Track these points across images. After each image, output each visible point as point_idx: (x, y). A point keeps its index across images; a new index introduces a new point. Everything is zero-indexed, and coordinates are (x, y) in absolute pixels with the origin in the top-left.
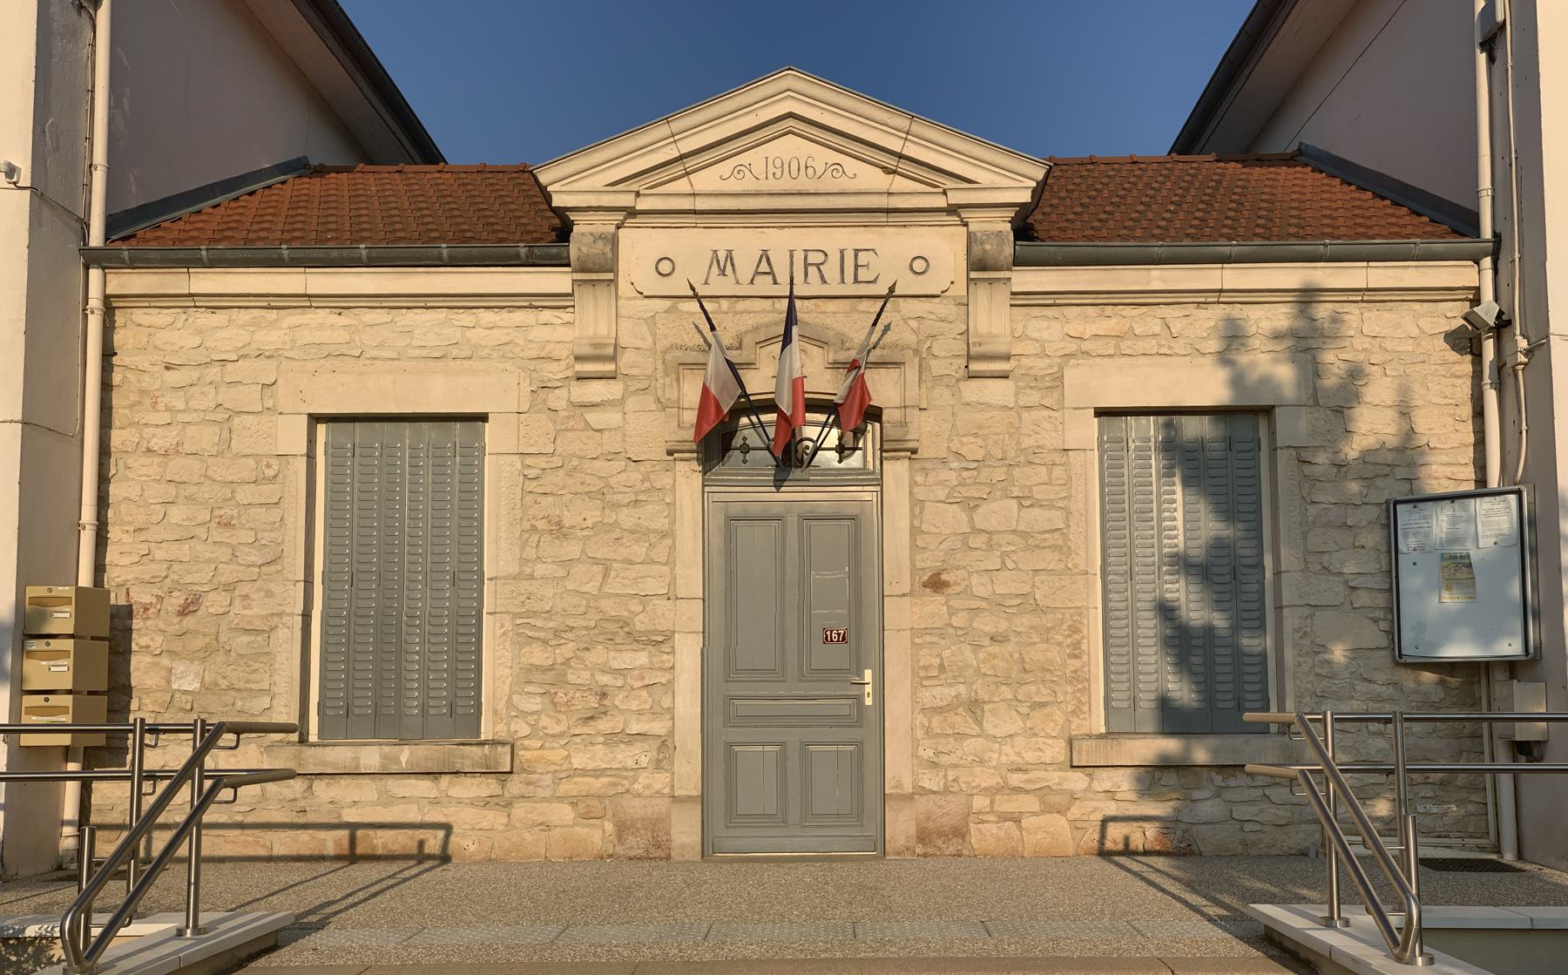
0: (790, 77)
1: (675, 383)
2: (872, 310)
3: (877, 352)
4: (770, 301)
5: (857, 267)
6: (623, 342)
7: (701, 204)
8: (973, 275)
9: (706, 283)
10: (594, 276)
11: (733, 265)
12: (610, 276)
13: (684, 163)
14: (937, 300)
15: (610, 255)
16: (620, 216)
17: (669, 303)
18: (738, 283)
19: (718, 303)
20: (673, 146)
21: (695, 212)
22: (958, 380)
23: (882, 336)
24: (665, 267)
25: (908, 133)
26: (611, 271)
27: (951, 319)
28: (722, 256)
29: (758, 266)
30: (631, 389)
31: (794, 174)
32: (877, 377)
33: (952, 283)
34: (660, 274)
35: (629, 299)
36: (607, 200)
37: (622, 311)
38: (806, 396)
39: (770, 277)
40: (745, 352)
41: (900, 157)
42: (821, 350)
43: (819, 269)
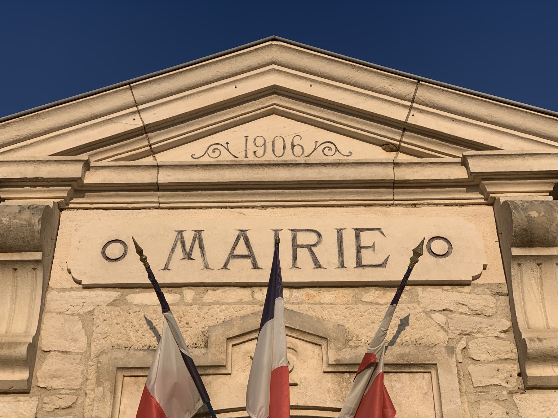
0: (274, 49)
1: (108, 395)
2: (381, 301)
3: (396, 350)
4: (248, 291)
5: (359, 248)
6: (45, 343)
7: (165, 177)
8: (516, 251)
9: (166, 268)
10: (16, 257)
11: (202, 247)
12: (38, 256)
13: (149, 139)
14: (467, 289)
15: (38, 227)
16: (63, 193)
17: (114, 294)
18: (207, 268)
19: (181, 294)
20: (137, 116)
21: (157, 187)
22: (511, 393)
23: (399, 332)
24: (114, 250)
25: (413, 101)
26: (37, 249)
27: (489, 312)
28: (188, 237)
29: (234, 248)
30: (49, 407)
31: (279, 152)
32: (399, 385)
33: (485, 267)
34: (107, 258)
35: (63, 290)
36: (45, 172)
37: (50, 305)
38: (293, 413)
39: (249, 260)
40: (212, 350)
41: (404, 130)
42: (317, 348)
43: (312, 253)
